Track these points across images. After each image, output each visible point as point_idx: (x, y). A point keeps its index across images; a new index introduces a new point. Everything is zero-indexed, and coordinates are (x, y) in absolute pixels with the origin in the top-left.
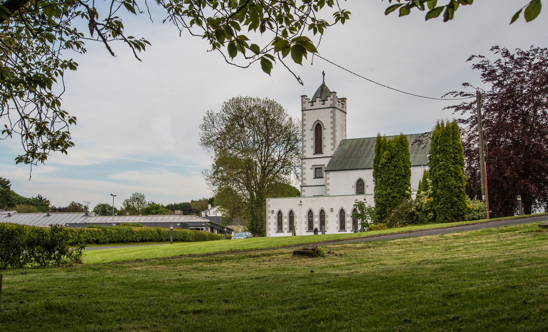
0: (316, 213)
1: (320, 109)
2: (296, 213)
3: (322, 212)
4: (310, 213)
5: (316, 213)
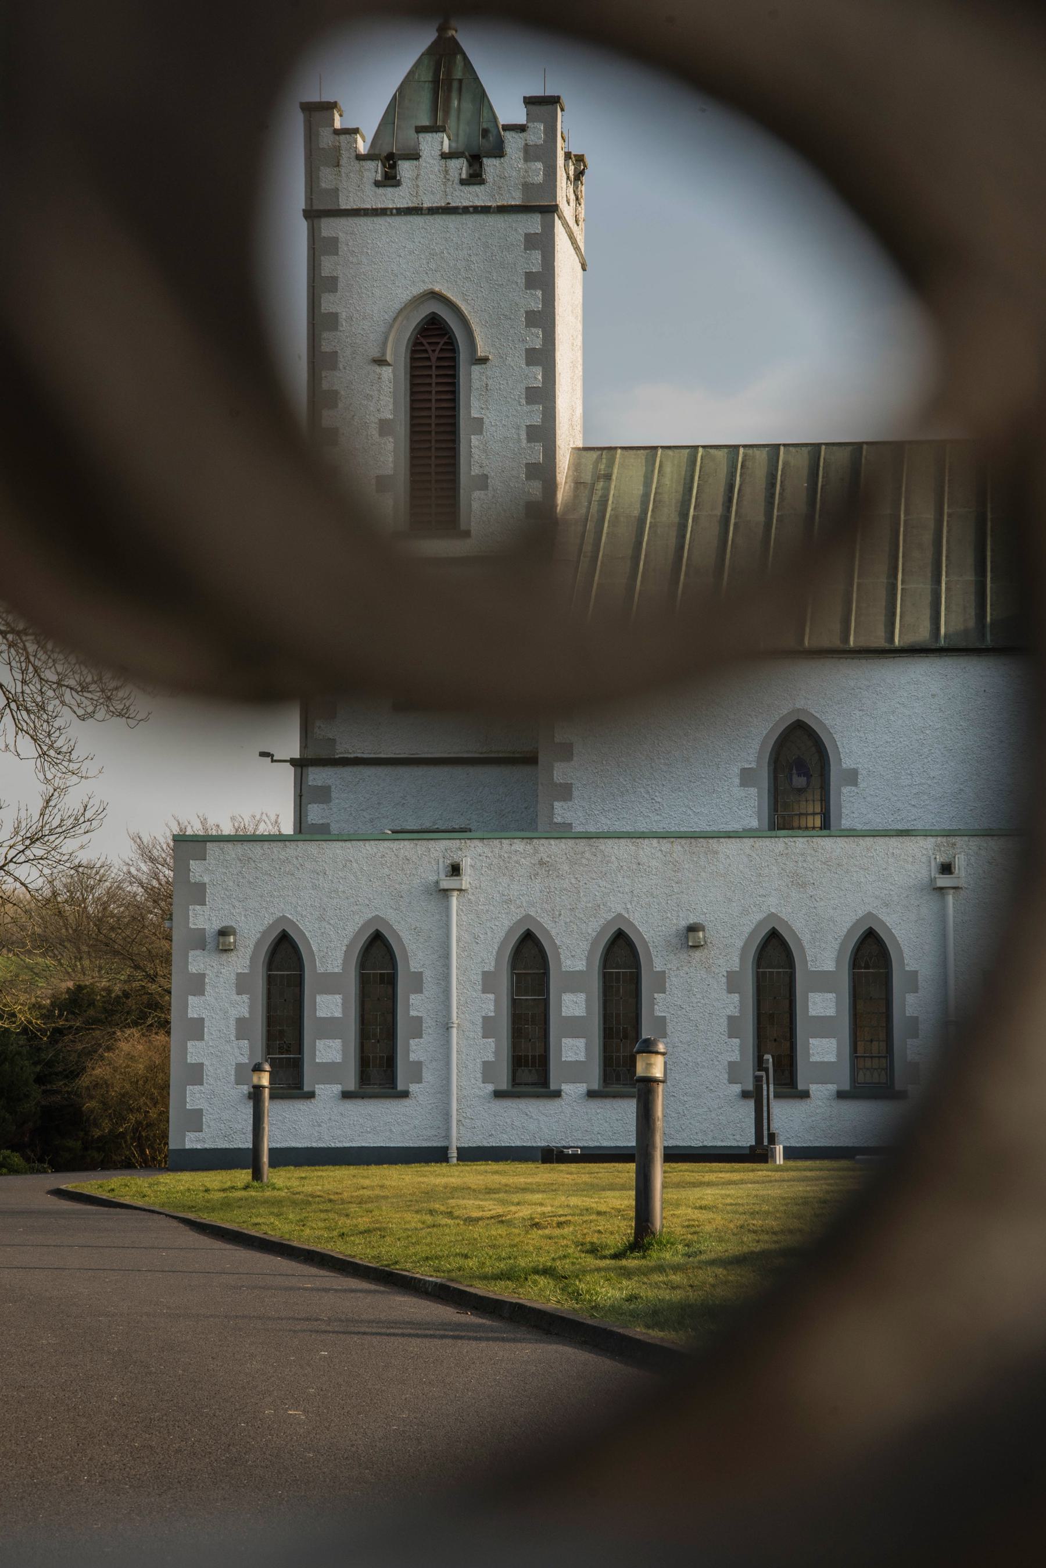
0: (574, 953)
1: (448, 210)
2: (415, 955)
3: (620, 954)
4: (528, 959)
5: (574, 953)
